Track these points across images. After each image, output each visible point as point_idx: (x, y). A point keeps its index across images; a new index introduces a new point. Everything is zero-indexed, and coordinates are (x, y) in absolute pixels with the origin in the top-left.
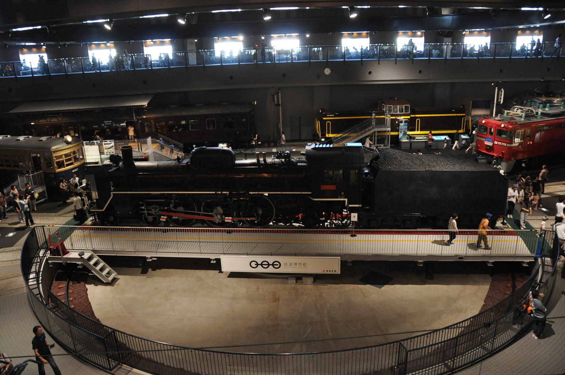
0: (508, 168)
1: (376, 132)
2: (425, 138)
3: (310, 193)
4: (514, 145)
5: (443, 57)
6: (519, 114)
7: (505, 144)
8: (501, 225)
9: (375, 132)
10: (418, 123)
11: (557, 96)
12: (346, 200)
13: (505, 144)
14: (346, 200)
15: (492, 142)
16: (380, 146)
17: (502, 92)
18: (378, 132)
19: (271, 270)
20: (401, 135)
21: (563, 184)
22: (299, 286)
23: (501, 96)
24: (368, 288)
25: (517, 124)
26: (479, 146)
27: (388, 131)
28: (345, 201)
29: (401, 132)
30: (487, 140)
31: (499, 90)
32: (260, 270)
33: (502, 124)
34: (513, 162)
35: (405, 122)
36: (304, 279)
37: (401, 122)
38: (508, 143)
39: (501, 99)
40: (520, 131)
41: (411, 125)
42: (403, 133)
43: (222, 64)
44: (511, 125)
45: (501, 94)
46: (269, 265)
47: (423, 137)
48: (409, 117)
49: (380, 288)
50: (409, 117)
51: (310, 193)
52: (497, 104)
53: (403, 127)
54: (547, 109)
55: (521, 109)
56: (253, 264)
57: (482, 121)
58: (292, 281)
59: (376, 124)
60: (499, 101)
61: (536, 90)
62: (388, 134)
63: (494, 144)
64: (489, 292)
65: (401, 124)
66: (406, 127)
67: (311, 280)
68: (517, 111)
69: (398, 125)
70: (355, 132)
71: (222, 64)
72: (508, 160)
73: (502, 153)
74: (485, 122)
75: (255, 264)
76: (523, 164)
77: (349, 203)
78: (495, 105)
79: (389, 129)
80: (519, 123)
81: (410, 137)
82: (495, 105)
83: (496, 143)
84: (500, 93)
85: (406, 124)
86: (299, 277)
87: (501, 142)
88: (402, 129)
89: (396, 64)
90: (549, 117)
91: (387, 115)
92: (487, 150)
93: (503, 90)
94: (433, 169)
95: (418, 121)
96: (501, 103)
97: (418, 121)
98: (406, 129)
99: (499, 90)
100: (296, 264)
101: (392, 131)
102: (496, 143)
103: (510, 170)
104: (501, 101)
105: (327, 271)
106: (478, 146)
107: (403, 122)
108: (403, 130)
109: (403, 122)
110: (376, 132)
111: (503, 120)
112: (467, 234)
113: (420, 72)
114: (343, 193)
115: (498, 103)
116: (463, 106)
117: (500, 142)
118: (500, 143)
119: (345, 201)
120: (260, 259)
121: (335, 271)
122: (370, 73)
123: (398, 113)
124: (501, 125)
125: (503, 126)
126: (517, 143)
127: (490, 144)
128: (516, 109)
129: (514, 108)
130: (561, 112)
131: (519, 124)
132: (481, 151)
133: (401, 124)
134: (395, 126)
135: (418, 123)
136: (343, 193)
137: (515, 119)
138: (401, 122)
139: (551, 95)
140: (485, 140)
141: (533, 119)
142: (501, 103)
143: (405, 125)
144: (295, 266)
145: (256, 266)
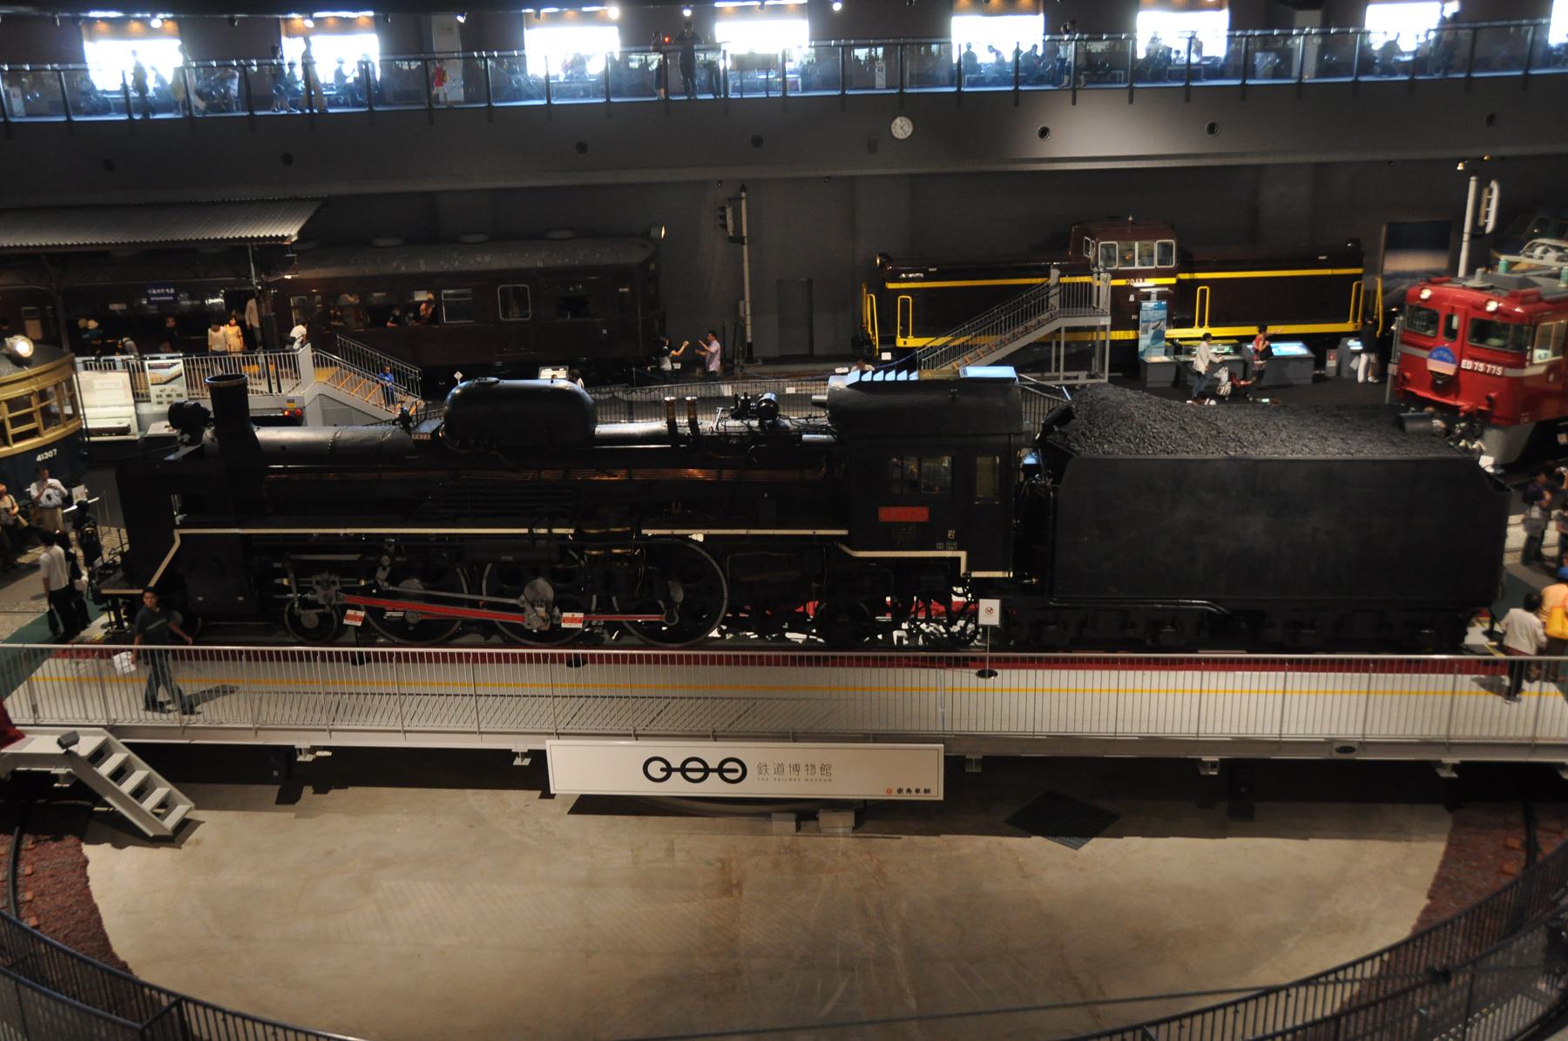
1: (1063, 330)
2: (1227, 349)
3: (844, 532)
4: (1529, 371)
5: (1289, 77)
6: (1549, 268)
7: (1499, 370)
8: (1484, 641)
9: (1059, 331)
10: (1203, 299)
12: (963, 555)
13: (1499, 370)
14: (963, 555)
15: (1453, 362)
16: (1076, 378)
17: (1491, 192)
18: (1069, 330)
19: (713, 787)
20: (1144, 342)
22: (804, 841)
23: (1488, 205)
24: (1037, 848)
25: (1540, 300)
26: (1408, 375)
27: (1104, 328)
28: (958, 559)
29: (1146, 331)
30: (1435, 355)
31: (1483, 185)
32: (677, 786)
33: (1489, 300)
34: (1526, 426)
35: (1160, 296)
36: (825, 818)
37: (1147, 297)
38: (1510, 366)
39: (1487, 216)
40: (1553, 325)
41: (1180, 306)
42: (1151, 332)
43: (549, 100)
44: (1521, 304)
45: (1489, 201)
46: (707, 770)
47: (1220, 346)
48: (1173, 281)
49: (1077, 847)
50: (1173, 281)
51: (844, 532)
52: (1473, 236)
53: (1151, 313)
55: (1559, 249)
56: (656, 769)
57: (1420, 292)
58: (784, 826)
59: (1064, 303)
60: (1481, 223)
62: (1102, 336)
63: (1459, 369)
64: (1443, 865)
65: (1144, 303)
66: (1163, 313)
67: (848, 819)
68: (1541, 258)
69: (1137, 308)
70: (995, 330)
71: (549, 100)
72: (1506, 422)
73: (1489, 398)
74: (1431, 298)
75: (662, 770)
77: (971, 566)
78: (1466, 237)
80: (1547, 298)
81: (1176, 348)
82: (1466, 237)
83: (1467, 364)
84: (1485, 196)
85: (1164, 303)
86: (806, 812)
87: (1487, 362)
88: (1148, 321)
89: (1131, 101)
91: (1099, 273)
92: (1435, 388)
93: (1494, 185)
94: (1253, 454)
95: (1203, 292)
96: (1489, 228)
97: (1203, 292)
98: (1161, 320)
99: (1483, 185)
100: (796, 768)
101: (1114, 327)
102: (1467, 364)
104: (1486, 224)
105: (900, 791)
106: (1404, 378)
107: (1154, 296)
108: (1152, 325)
109: (1154, 296)
110: (1063, 330)
111: (1492, 287)
112: (1366, 671)
113: (1212, 129)
114: (951, 534)
115: (1477, 229)
116: (1356, 241)
117: (1480, 360)
118: (1480, 366)
119: (958, 559)
120: (676, 752)
121: (927, 791)
122: (1044, 133)
123: (1137, 267)
124: (1485, 304)
125: (1492, 306)
126: (1541, 364)
127: (1448, 369)
128: (1538, 251)
129: (1532, 248)
131: (1549, 302)
132: (1414, 393)
133: (1144, 303)
134: (1125, 310)
135: (1203, 299)
136: (951, 534)
137: (1534, 285)
138: (1147, 297)
140: (1430, 357)
142: (1489, 228)
144: (794, 776)
145: (665, 774)
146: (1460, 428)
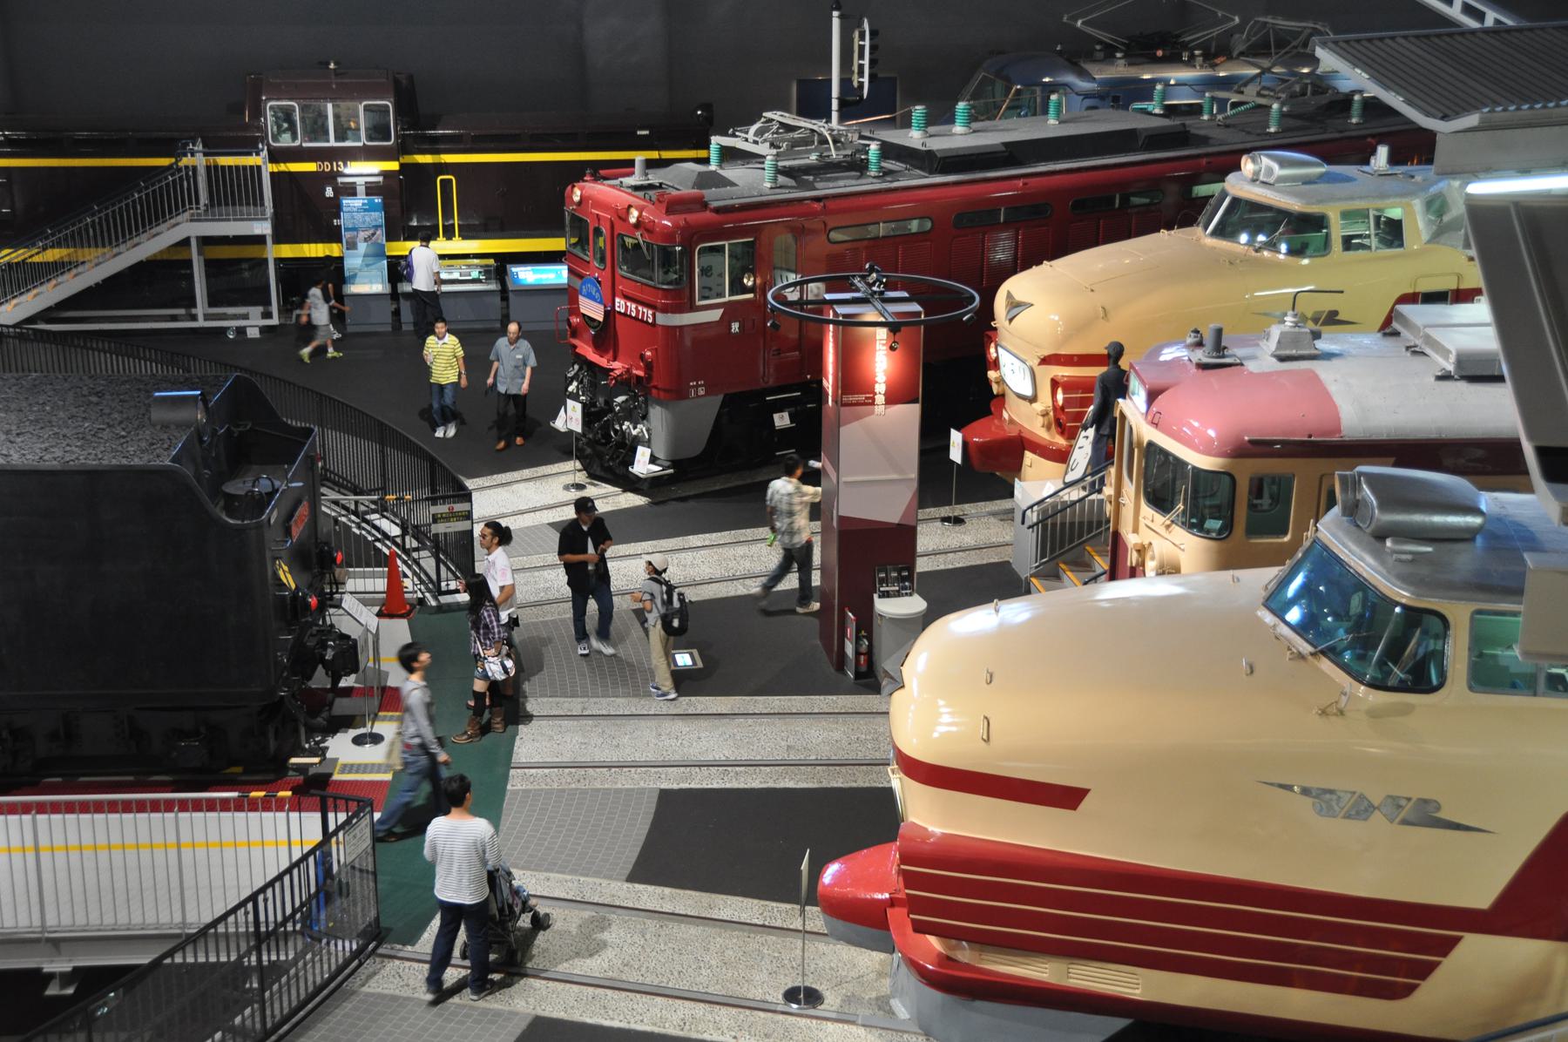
0: (677, 437)
1: (194, 243)
2: (475, 274)
9: (185, 242)
11: (1192, 57)
16: (246, 317)
18: (205, 241)
20: (353, 262)
21: (944, 520)
23: (861, 57)
34: (704, 406)
35: (371, 190)
37: (351, 191)
38: (665, 310)
47: (465, 270)
48: (393, 166)
50: (393, 166)
53: (358, 216)
54: (958, 128)
59: (215, 200)
61: (1079, 23)
63: (610, 314)
65: (346, 202)
66: (378, 217)
69: (335, 208)
70: (97, 242)
72: (676, 393)
76: (776, 416)
79: (264, 228)
83: (620, 304)
85: (378, 200)
88: (355, 229)
90: (933, 171)
98: (376, 227)
101: (281, 237)
103: (697, 447)
107: (361, 190)
108: (362, 235)
110: (194, 243)
116: (707, 107)
123: (332, 143)
130: (1006, 144)
131: (717, 210)
133: (346, 202)
138: (351, 191)
139: (1160, 53)
141: (837, 179)
143: (370, 208)
146: (619, 405)
